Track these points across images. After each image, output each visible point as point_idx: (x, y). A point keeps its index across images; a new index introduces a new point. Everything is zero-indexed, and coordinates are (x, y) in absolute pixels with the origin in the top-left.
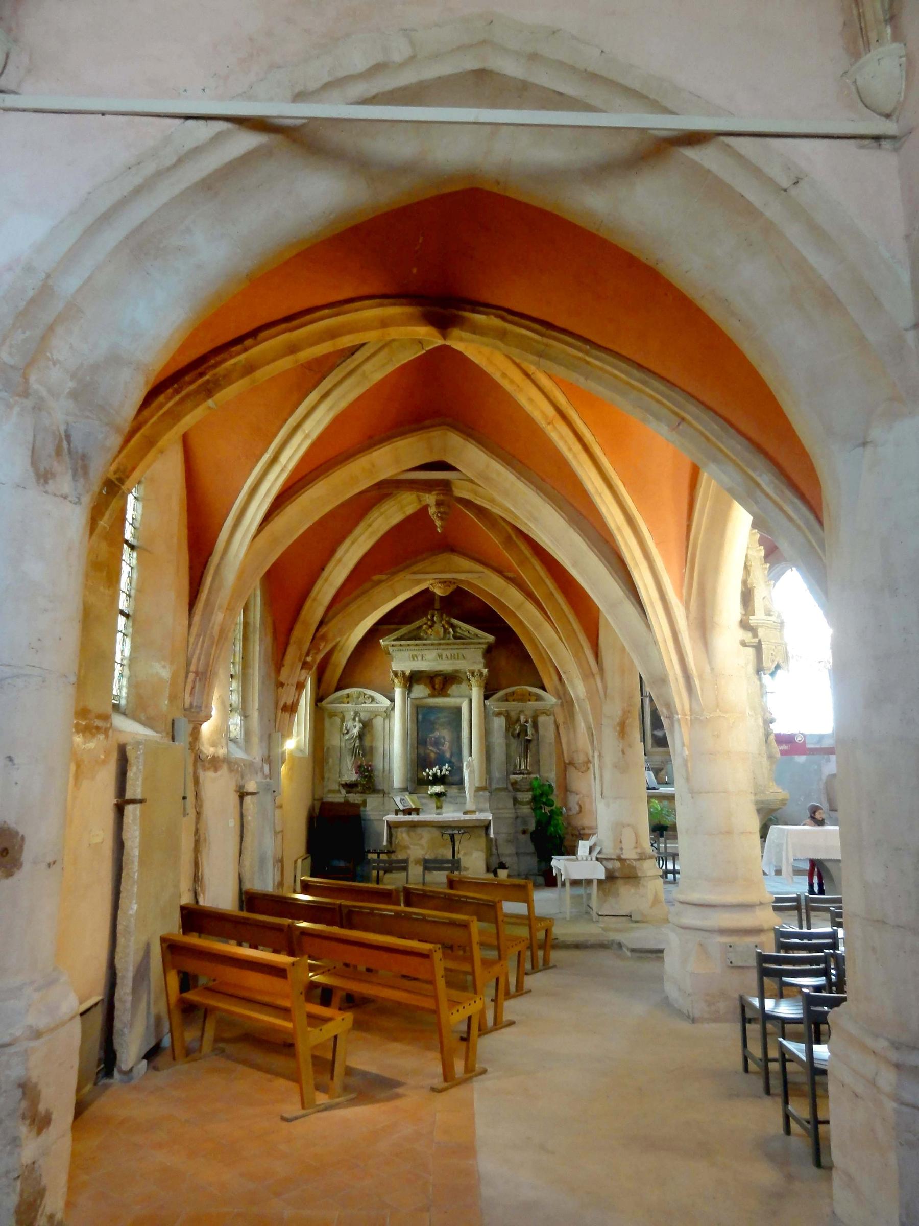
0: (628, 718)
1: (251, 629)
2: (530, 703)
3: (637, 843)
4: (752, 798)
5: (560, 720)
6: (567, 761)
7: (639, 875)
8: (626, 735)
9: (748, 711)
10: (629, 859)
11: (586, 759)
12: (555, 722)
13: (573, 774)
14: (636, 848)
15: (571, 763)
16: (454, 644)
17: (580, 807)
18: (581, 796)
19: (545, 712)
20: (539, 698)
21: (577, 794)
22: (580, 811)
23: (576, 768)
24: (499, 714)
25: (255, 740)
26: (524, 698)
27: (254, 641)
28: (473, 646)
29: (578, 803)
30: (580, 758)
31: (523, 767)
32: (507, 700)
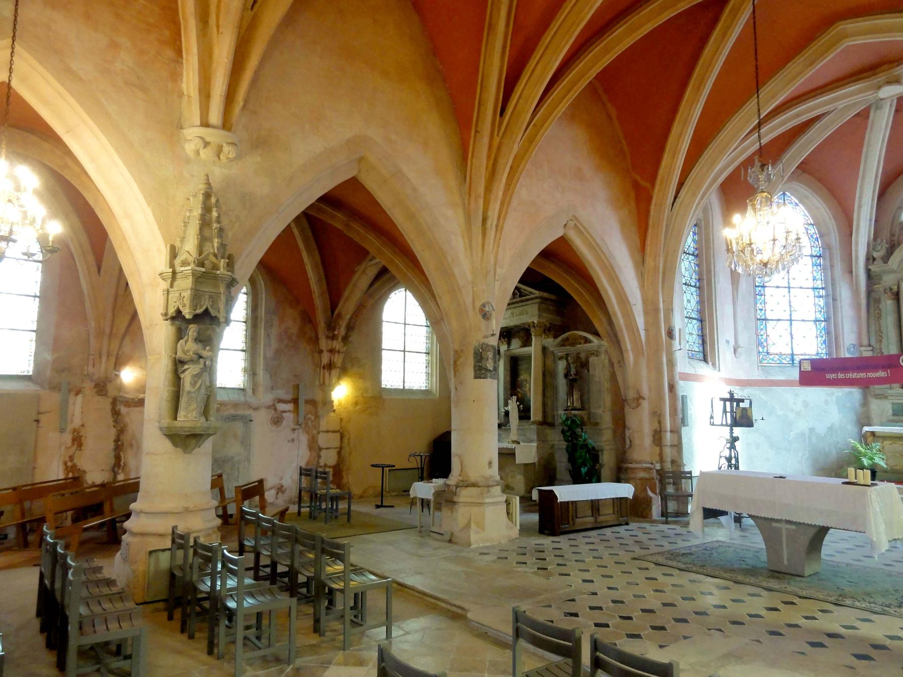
0: (460, 357)
1: (259, 318)
2: (579, 346)
3: (462, 471)
4: (157, 424)
5: (615, 361)
6: (624, 398)
7: (455, 499)
8: (457, 373)
9: (164, 353)
10: (452, 485)
11: (636, 396)
12: (610, 361)
13: (627, 410)
14: (460, 475)
15: (626, 400)
16: (522, 301)
17: (630, 441)
18: (631, 431)
19: (596, 353)
20: (587, 341)
21: (629, 429)
22: (631, 446)
23: (629, 405)
24: (561, 358)
25: (261, 389)
26: (573, 342)
27: (261, 327)
28: (530, 302)
29: (629, 438)
30: (631, 394)
31: (569, 404)
32: (565, 346)
